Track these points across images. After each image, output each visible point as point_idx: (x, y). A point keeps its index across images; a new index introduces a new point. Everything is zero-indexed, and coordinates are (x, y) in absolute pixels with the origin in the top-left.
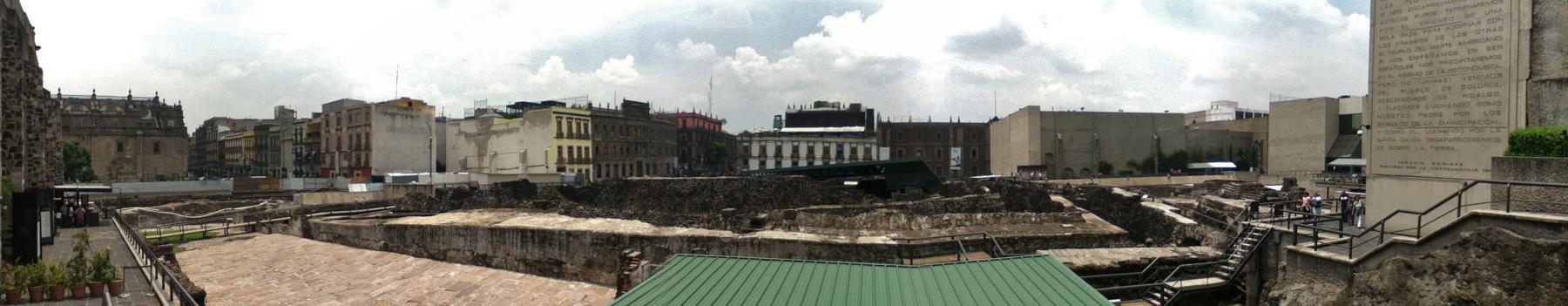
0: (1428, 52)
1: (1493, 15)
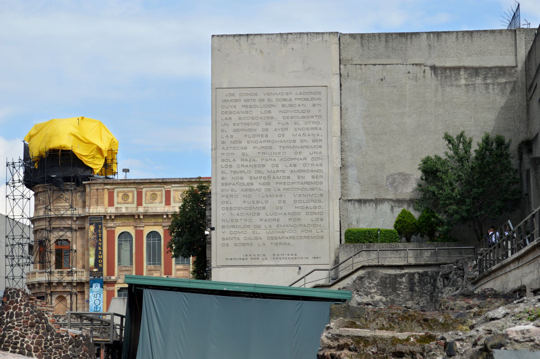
0: (266, 175)
1: (315, 156)
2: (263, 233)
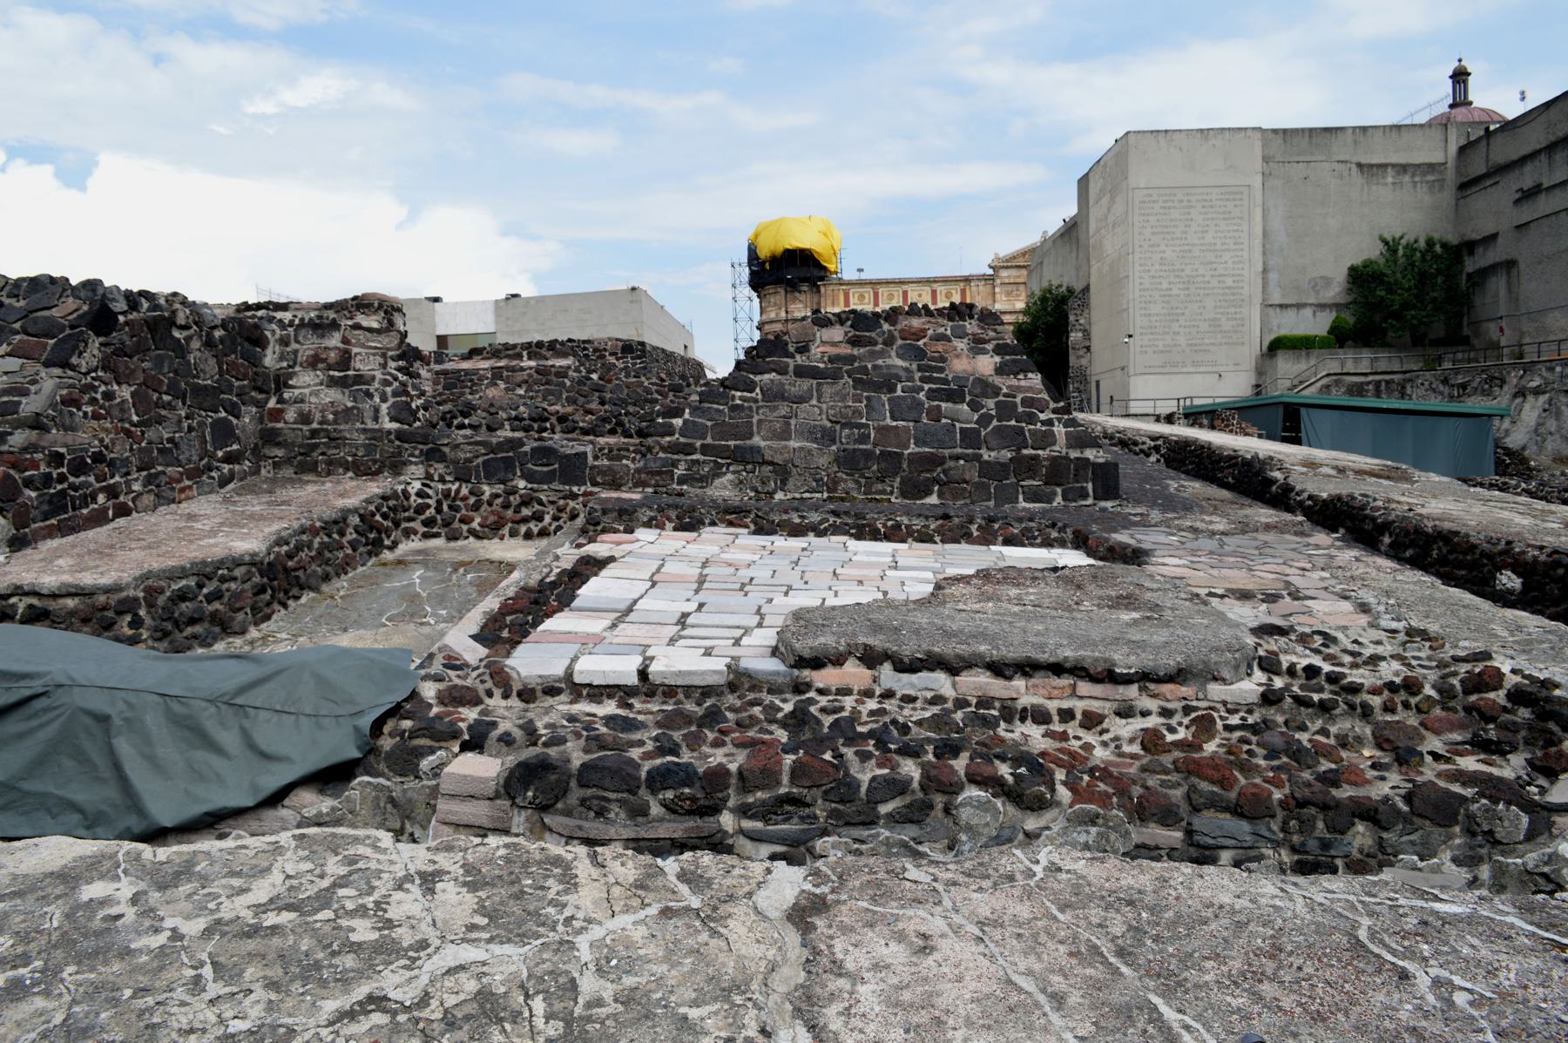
0: (1185, 279)
2: (1182, 340)
